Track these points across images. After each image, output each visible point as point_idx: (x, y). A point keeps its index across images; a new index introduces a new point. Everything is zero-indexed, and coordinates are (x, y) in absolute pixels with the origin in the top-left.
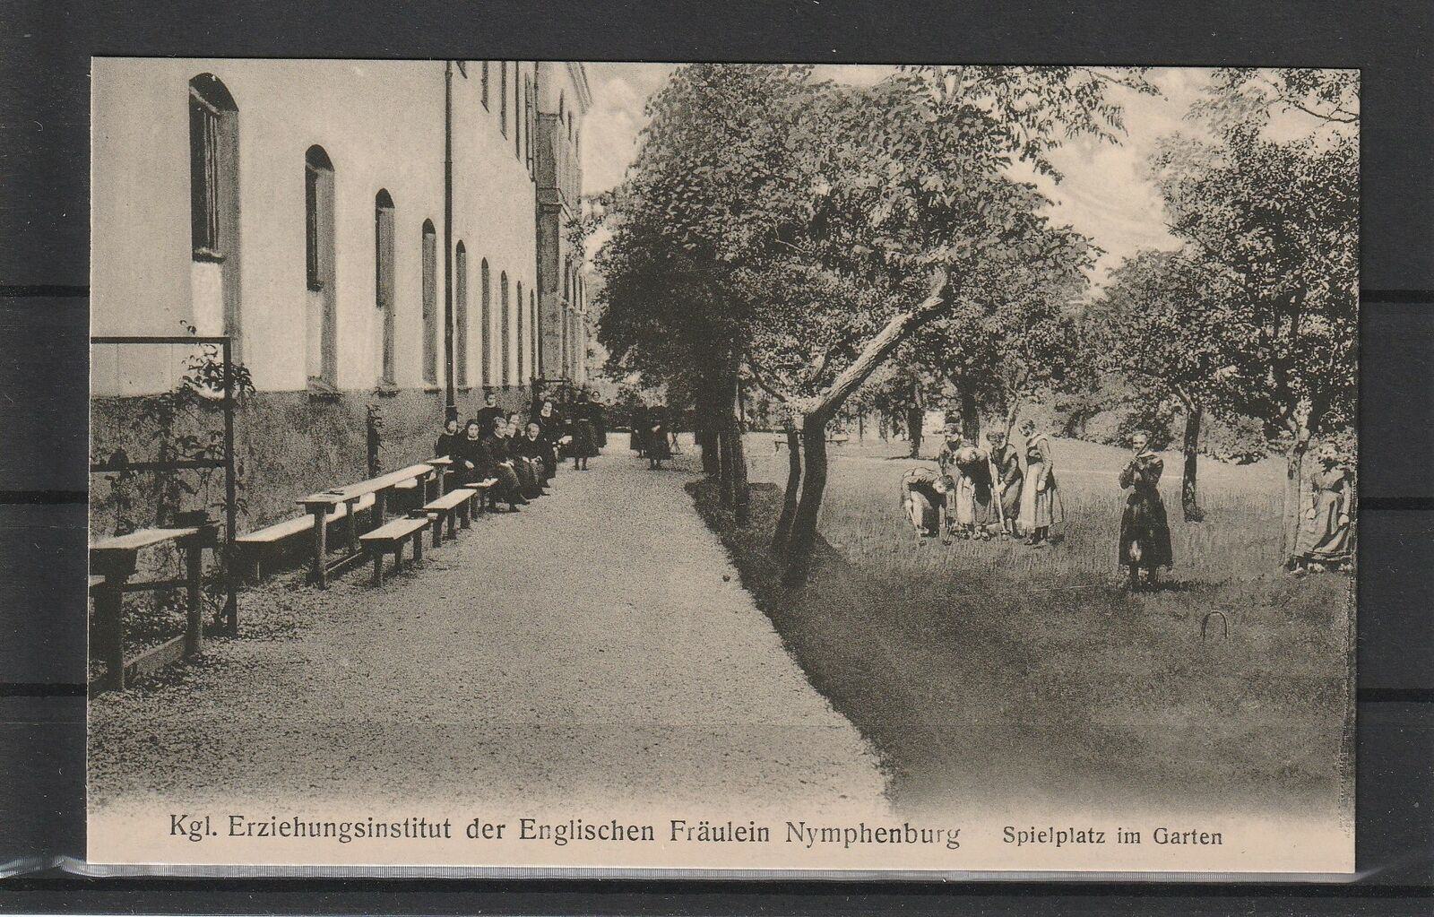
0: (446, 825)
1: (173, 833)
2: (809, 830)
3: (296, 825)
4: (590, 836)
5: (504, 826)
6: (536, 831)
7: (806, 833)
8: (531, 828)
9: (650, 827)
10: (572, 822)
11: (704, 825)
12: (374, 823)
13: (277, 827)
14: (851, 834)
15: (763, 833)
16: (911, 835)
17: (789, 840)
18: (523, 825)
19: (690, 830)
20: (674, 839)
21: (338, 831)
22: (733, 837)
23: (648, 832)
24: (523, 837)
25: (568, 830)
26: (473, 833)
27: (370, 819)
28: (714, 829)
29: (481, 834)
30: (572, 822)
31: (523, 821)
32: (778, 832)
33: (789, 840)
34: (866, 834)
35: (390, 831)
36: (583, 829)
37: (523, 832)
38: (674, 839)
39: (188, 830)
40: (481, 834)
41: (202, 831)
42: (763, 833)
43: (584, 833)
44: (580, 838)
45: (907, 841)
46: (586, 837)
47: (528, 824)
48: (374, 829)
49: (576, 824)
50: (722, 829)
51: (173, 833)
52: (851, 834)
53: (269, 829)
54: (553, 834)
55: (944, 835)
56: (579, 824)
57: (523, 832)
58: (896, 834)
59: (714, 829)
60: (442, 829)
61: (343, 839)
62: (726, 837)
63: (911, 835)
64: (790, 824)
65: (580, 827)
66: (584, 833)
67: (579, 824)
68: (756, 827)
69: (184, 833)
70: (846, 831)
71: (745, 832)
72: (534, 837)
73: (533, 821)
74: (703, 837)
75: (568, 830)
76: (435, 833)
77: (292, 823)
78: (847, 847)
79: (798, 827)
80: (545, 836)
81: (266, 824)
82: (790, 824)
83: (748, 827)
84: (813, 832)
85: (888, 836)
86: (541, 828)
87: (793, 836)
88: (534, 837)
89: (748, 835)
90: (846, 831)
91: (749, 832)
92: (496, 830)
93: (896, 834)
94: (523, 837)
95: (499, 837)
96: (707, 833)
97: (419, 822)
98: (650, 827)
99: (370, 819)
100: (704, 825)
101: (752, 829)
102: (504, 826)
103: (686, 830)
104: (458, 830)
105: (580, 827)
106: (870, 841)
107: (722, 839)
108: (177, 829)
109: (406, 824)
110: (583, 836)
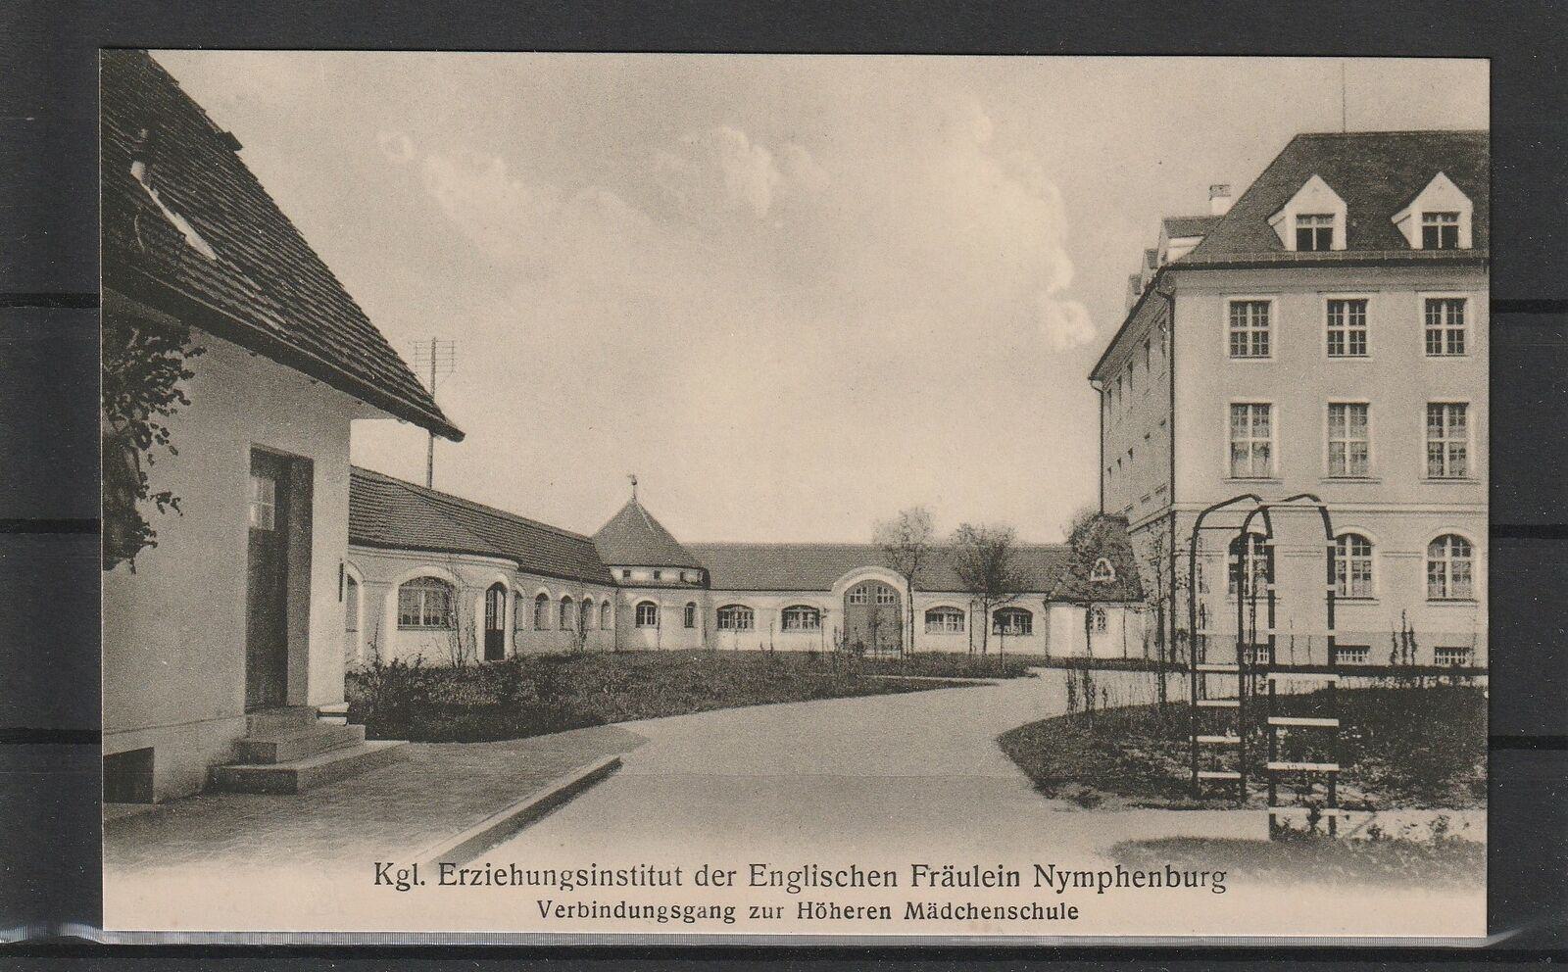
1: (378, 883)
2: (1060, 873)
3: (513, 873)
4: (827, 882)
5: (735, 873)
6: (767, 877)
7: (1056, 880)
8: (762, 874)
9: (1017, 873)
10: (806, 867)
11: (949, 869)
12: (1005, 871)
14: (1105, 878)
15: (1013, 877)
16: (1173, 877)
17: (1038, 885)
18: (753, 870)
19: (933, 874)
20: (915, 885)
24: (753, 884)
26: (701, 880)
27: (488, 865)
28: (959, 874)
29: (710, 881)
30: (806, 867)
31: (915, 867)
32: (1028, 877)
33: (1038, 885)
35: (615, 878)
36: (818, 876)
37: (753, 879)
38: (915, 885)
39: (394, 879)
40: (710, 881)
41: (410, 881)
42: (1013, 877)
44: (815, 885)
45: (1168, 884)
46: (618, 883)
47: (758, 869)
49: (811, 870)
50: (968, 874)
51: (378, 883)
52: (1105, 878)
53: (483, 877)
54: (786, 881)
56: (1000, 870)
57: (753, 879)
59: (959, 874)
61: (791, 889)
63: (1173, 880)
64: (1038, 867)
65: (815, 873)
66: (819, 879)
67: (1000, 870)
69: (389, 882)
70: (1100, 874)
71: (993, 877)
72: (765, 884)
73: (764, 866)
74: (947, 882)
78: (1101, 892)
81: (480, 872)
82: (1038, 867)
83: (996, 871)
84: (1064, 876)
85: (1147, 881)
86: (772, 873)
87: (1042, 880)
88: (765, 884)
90: (1100, 874)
91: (997, 876)
92: (726, 875)
93: (1155, 877)
95: (730, 884)
96: (951, 878)
97: (646, 869)
98: (894, 873)
99: (488, 865)
100: (949, 869)
101: (1000, 874)
102: (735, 873)
103: (929, 877)
104: (687, 877)
105: (815, 873)
106: (977, 885)
107: (1195, 885)
108: (382, 878)
109: (633, 871)
110: (818, 883)
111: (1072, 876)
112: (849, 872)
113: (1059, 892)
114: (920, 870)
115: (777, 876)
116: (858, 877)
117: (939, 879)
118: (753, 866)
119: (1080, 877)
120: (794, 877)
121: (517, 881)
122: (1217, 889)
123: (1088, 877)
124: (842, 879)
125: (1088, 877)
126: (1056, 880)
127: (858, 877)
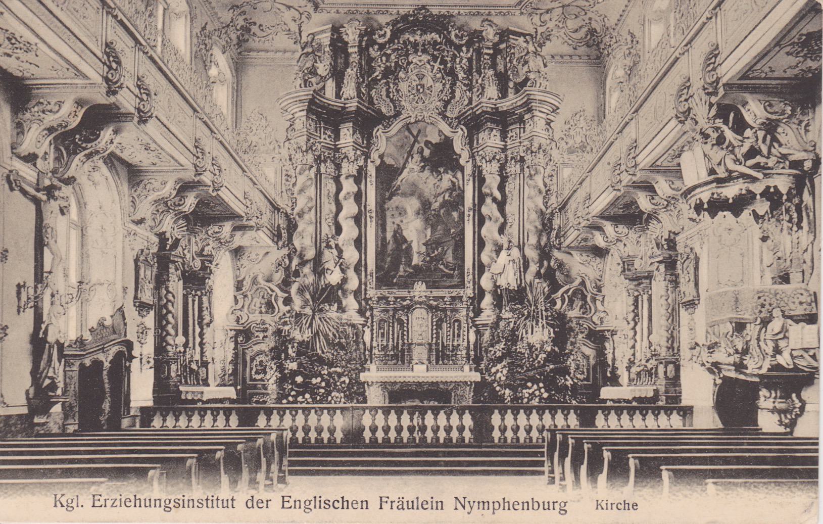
0: (233, 500)
1: (55, 506)
4: (327, 507)
7: (467, 503)
12: (434, 500)
13: (123, 500)
14: (496, 505)
20: (381, 508)
21: (163, 504)
22: (420, 507)
23: (364, 504)
24: (283, 507)
25: (313, 503)
26: (250, 504)
32: (449, 503)
34: (507, 505)
35: (196, 504)
38: (381, 508)
39: (65, 504)
41: (74, 505)
42: (440, 504)
43: (323, 505)
47: (286, 499)
48: (434, 505)
49: (318, 499)
51: (55, 506)
53: (117, 503)
55: (557, 506)
58: (526, 505)
60: (230, 502)
62: (415, 507)
63: (536, 505)
66: (323, 505)
68: (405, 501)
69: (62, 506)
75: (313, 503)
76: (225, 505)
77: (133, 498)
78: (494, 513)
79: (462, 500)
80: (297, 506)
83: (429, 500)
84: (472, 503)
87: (459, 506)
89: (429, 506)
94: (283, 507)
97: (215, 498)
103: (389, 503)
108: (58, 503)
109: (207, 500)
111: (476, 504)
112: (341, 500)
113: (469, 513)
114: (384, 500)
115: (298, 503)
116: (345, 503)
117: (395, 505)
118: (283, 497)
119: (481, 504)
120: (307, 503)
121: (138, 504)
122: (563, 512)
123: (486, 504)
124: (336, 505)
125: (486, 504)
126: (467, 506)
127: (345, 503)
